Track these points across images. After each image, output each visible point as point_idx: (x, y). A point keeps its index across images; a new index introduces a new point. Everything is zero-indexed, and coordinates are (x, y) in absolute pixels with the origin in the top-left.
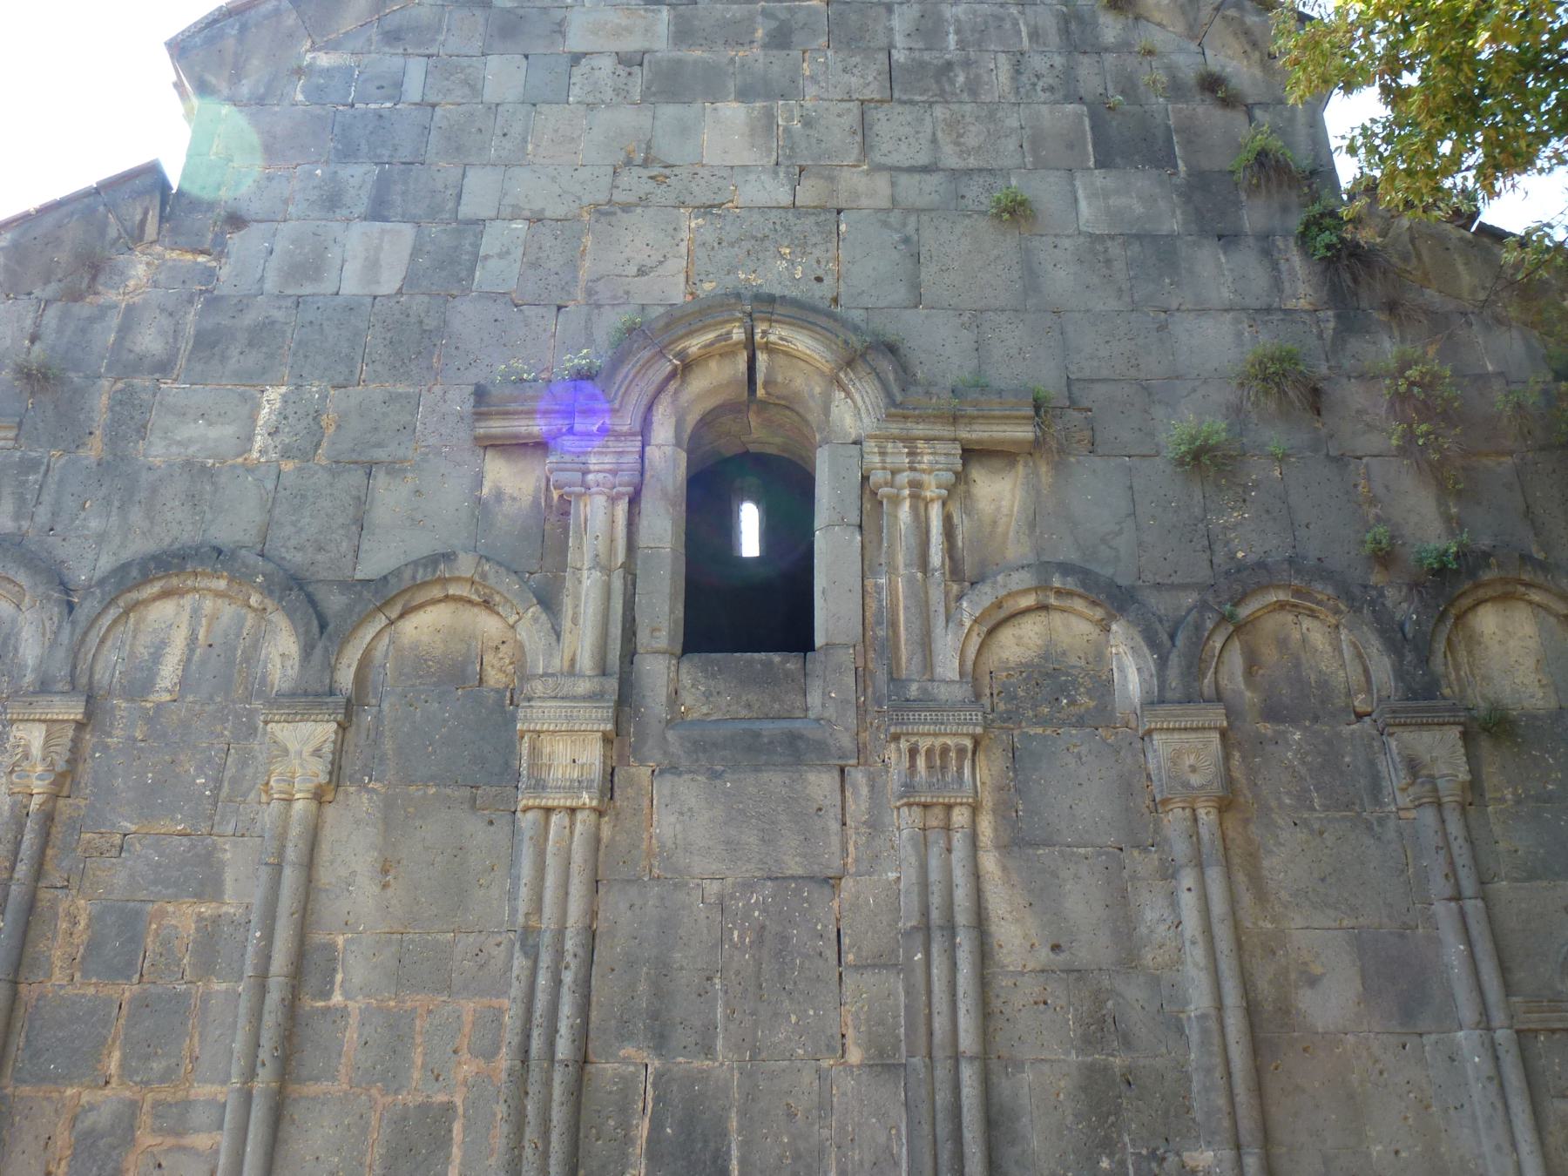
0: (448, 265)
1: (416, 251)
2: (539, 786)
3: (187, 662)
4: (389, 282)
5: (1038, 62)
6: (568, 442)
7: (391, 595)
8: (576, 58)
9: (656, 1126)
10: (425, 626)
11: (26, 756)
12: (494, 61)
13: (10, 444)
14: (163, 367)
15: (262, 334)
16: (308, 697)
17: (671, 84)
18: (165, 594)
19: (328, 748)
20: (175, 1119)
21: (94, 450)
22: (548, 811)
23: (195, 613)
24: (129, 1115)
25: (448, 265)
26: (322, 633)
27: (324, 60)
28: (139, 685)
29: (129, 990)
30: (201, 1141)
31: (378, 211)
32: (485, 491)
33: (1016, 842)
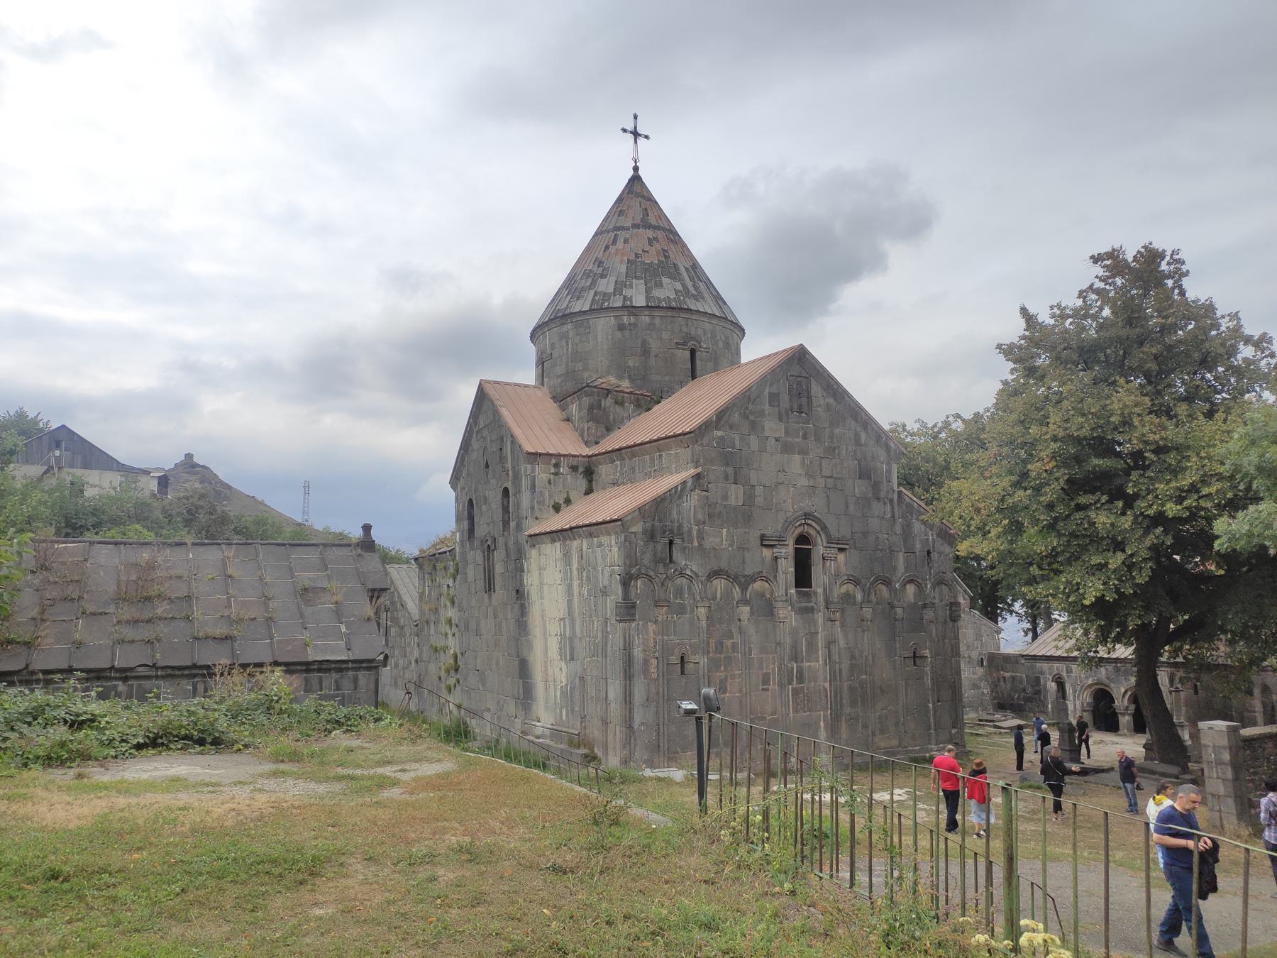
0: (750, 498)
5: (850, 449)
7: (752, 579)
10: (758, 585)
12: (752, 437)
14: (704, 523)
15: (720, 514)
16: (745, 602)
17: (787, 448)
20: (733, 677)
21: (696, 544)
24: (726, 678)
25: (750, 498)
26: (744, 588)
27: (719, 433)
28: (714, 598)
33: (842, 626)
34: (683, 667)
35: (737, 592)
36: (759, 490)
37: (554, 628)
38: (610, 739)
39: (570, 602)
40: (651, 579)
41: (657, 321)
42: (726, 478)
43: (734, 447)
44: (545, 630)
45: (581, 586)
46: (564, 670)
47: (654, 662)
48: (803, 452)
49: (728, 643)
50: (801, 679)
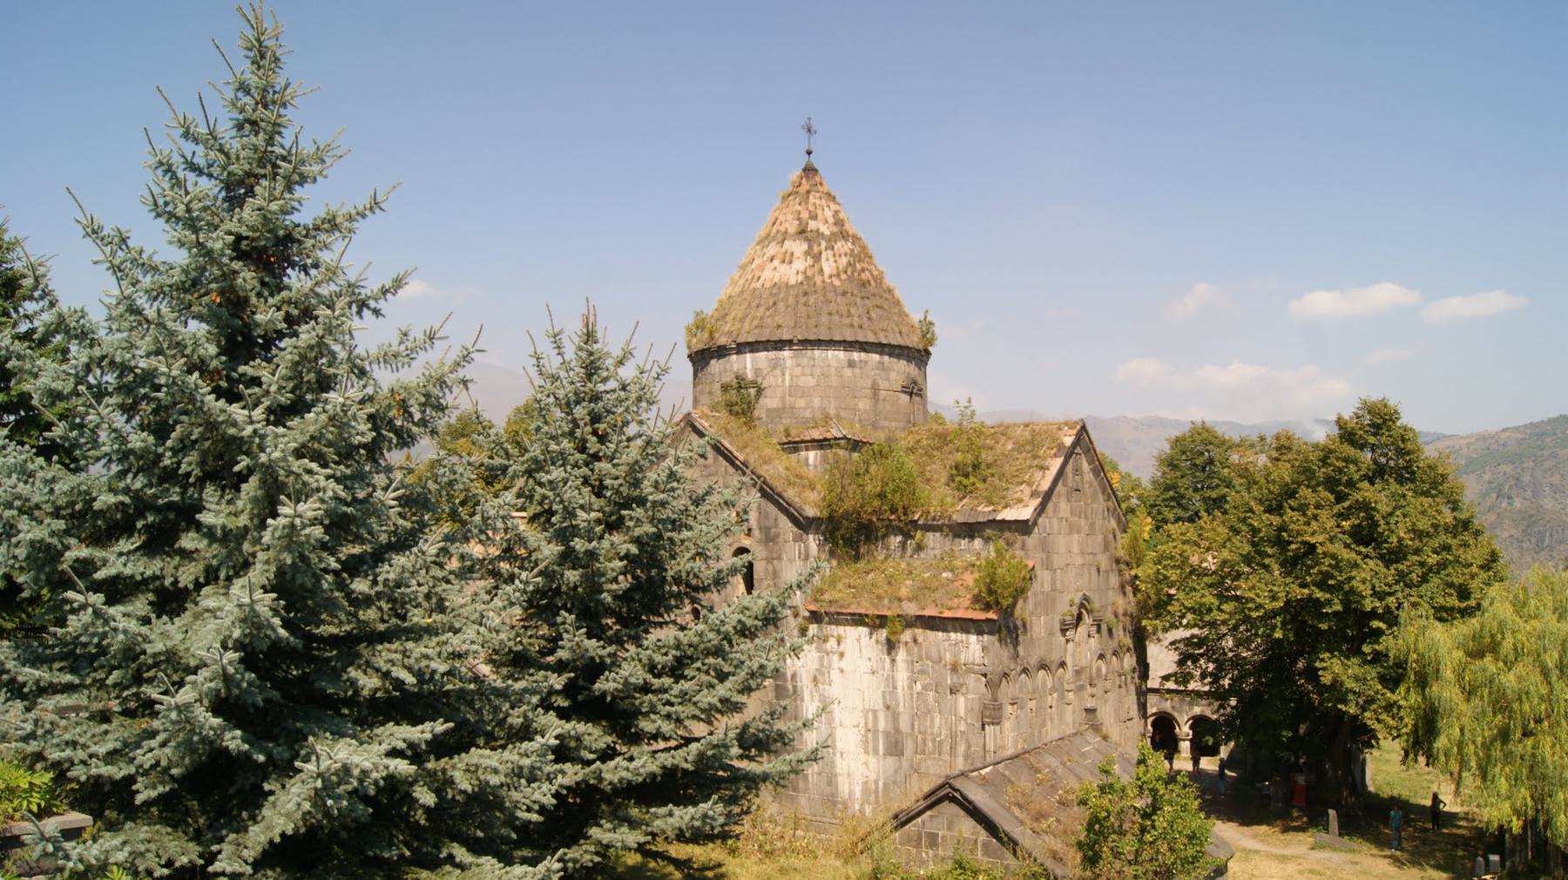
41: (886, 358)
48: (1079, 532)
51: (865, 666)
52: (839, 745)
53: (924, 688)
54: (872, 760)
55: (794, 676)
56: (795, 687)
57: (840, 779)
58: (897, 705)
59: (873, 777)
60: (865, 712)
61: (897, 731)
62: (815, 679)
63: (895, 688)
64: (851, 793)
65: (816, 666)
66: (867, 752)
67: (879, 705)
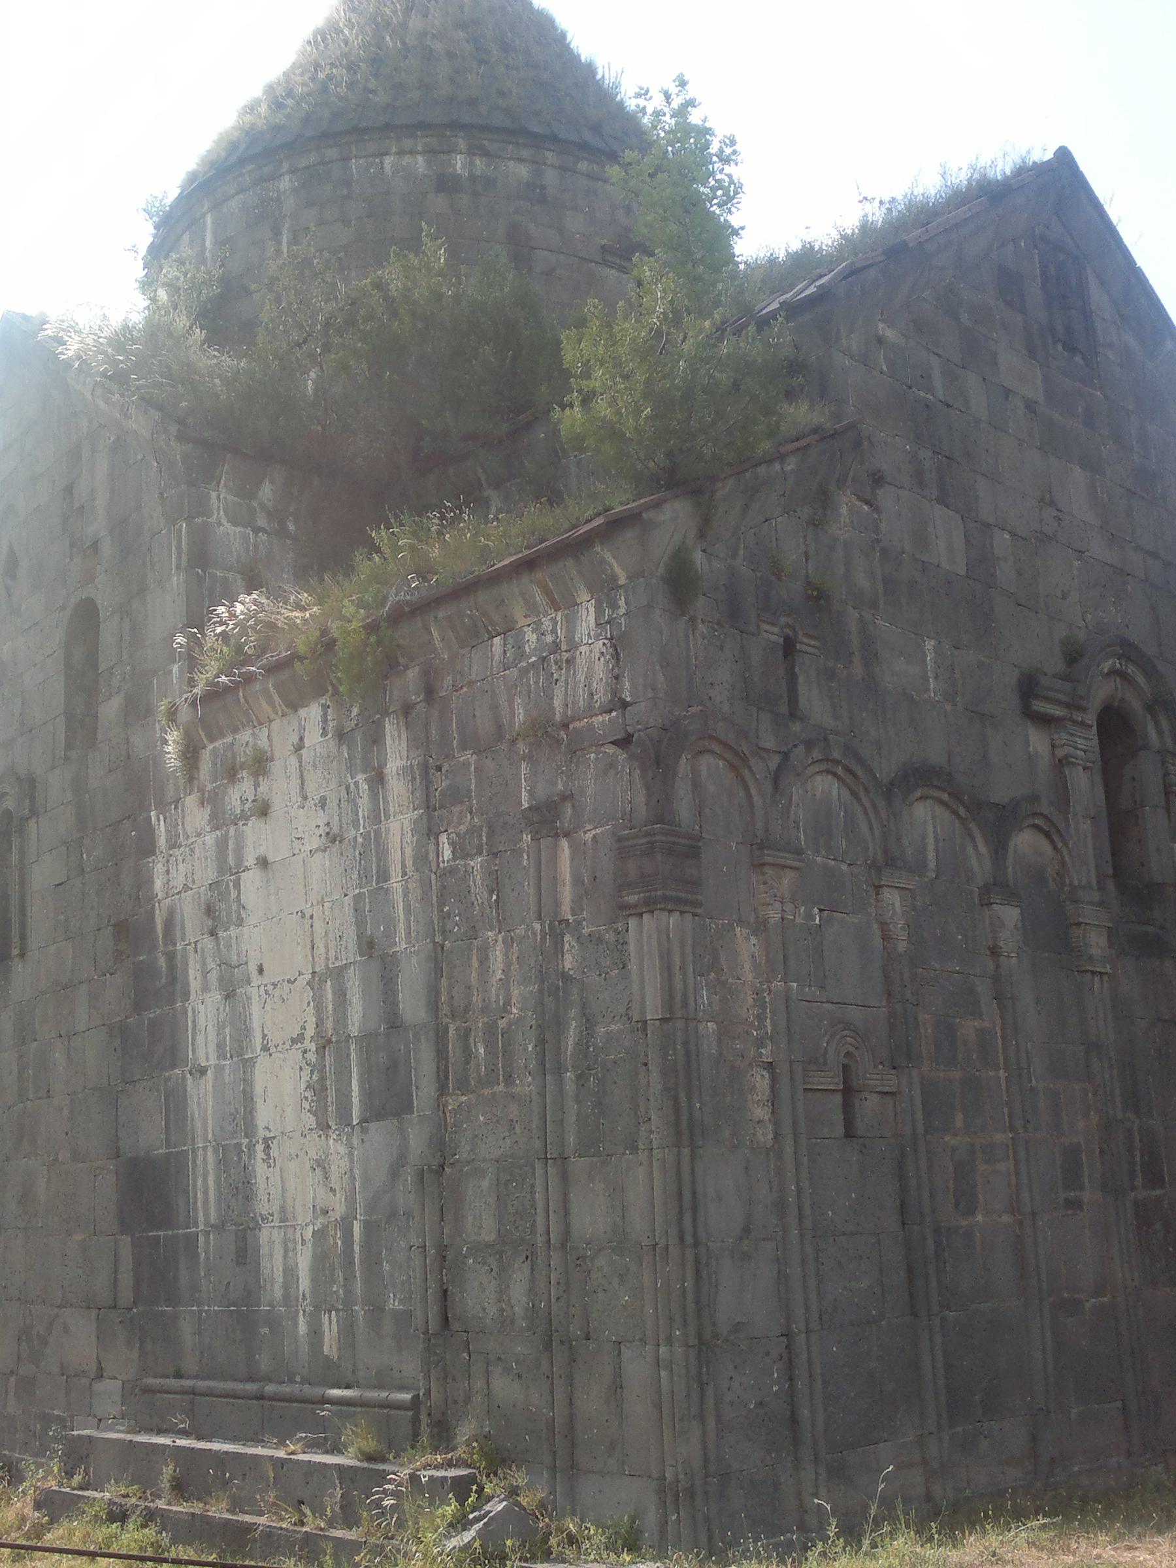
1: (968, 542)
2: (1091, 958)
3: (937, 850)
4: (962, 570)
6: (1069, 724)
8: (1008, 392)
9: (1142, 1157)
11: (894, 911)
13: (816, 652)
14: (874, 605)
18: (923, 798)
19: (1020, 925)
21: (858, 668)
22: (1093, 973)
23: (934, 817)
26: (999, 847)
29: (957, 1074)
30: (1001, 1167)
31: (942, 501)
32: (1031, 749)
34: (848, 1109)
35: (978, 858)
36: (1002, 542)
37: (282, 1016)
38: (591, 1402)
39: (370, 905)
40: (738, 762)
42: (919, 477)
43: (930, 389)
44: (243, 1032)
45: (429, 831)
46: (338, 1165)
47: (761, 1081)
49: (968, 1028)
50: (1155, 1179)
51: (310, 824)
52: (264, 1116)
53: (460, 851)
54: (336, 1148)
55: (169, 924)
56: (171, 957)
57: (264, 1235)
58: (390, 935)
59: (339, 1207)
60: (316, 981)
61: (394, 1023)
62: (210, 911)
63: (384, 876)
64: (290, 1272)
65: (211, 875)
66: (323, 1126)
67: (350, 953)
